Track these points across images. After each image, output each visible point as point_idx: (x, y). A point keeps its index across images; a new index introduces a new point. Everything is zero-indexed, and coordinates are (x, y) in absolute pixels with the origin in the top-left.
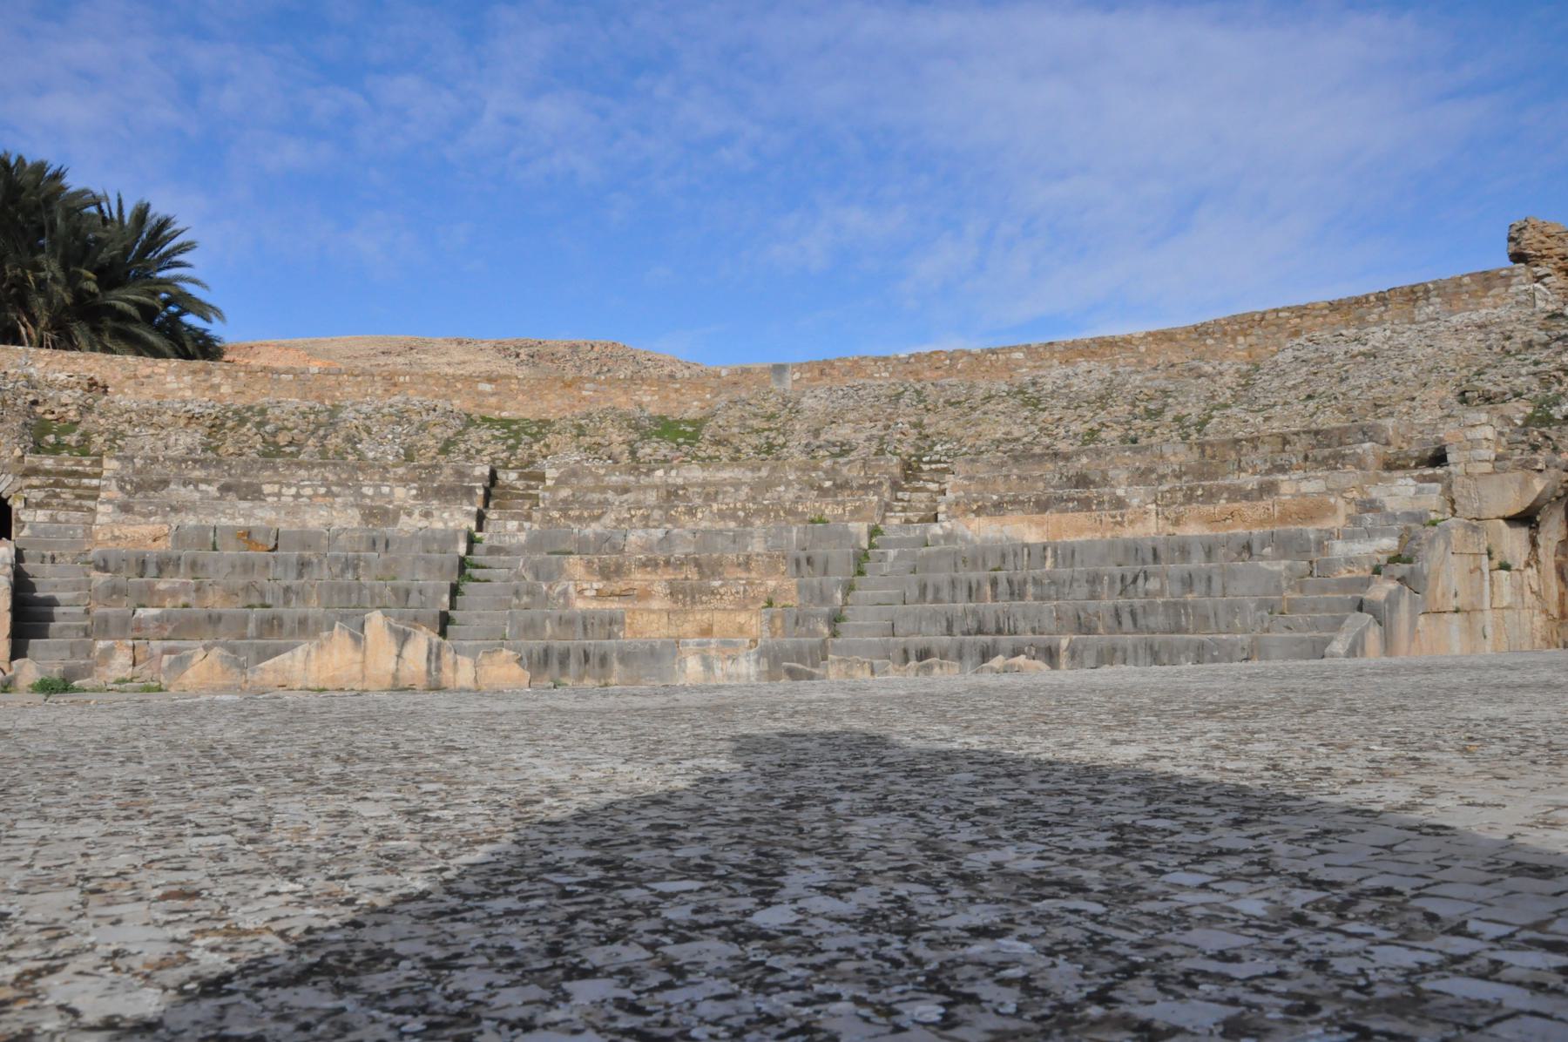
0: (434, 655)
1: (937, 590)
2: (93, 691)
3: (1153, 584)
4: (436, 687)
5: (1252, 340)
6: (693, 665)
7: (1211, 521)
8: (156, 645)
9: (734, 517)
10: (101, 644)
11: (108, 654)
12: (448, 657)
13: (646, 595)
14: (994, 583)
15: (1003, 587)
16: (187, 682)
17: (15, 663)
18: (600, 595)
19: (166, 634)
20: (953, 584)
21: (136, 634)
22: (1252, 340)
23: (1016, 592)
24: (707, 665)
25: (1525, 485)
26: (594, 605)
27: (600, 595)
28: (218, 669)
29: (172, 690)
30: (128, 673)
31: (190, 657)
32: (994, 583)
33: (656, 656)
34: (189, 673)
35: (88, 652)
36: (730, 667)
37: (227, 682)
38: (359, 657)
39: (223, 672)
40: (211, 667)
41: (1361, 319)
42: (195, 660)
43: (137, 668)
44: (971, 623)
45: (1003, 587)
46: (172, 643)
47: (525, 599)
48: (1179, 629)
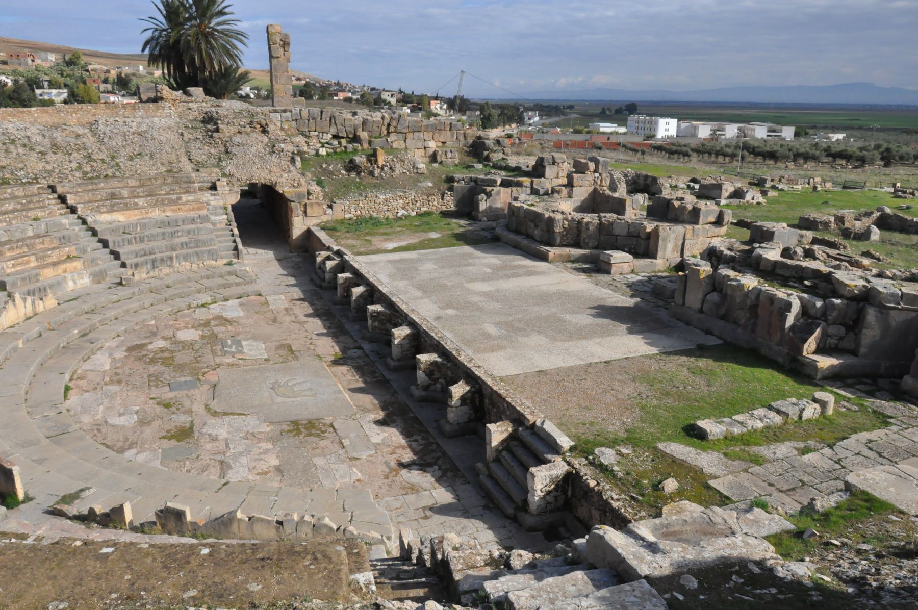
0: (33, 303)
3: (180, 234)
4: (36, 314)
5: (78, 116)
6: (71, 284)
7: (173, 211)
9: (5, 221)
12: (36, 303)
13: (28, 262)
14: (135, 238)
15: (138, 239)
18: (14, 266)
20: (123, 240)
22: (78, 116)
23: (142, 240)
24: (75, 283)
26: (13, 270)
27: (14, 266)
32: (135, 238)
33: (58, 284)
36: (82, 282)
41: (117, 113)
44: (142, 253)
45: (138, 239)
48: (198, 247)
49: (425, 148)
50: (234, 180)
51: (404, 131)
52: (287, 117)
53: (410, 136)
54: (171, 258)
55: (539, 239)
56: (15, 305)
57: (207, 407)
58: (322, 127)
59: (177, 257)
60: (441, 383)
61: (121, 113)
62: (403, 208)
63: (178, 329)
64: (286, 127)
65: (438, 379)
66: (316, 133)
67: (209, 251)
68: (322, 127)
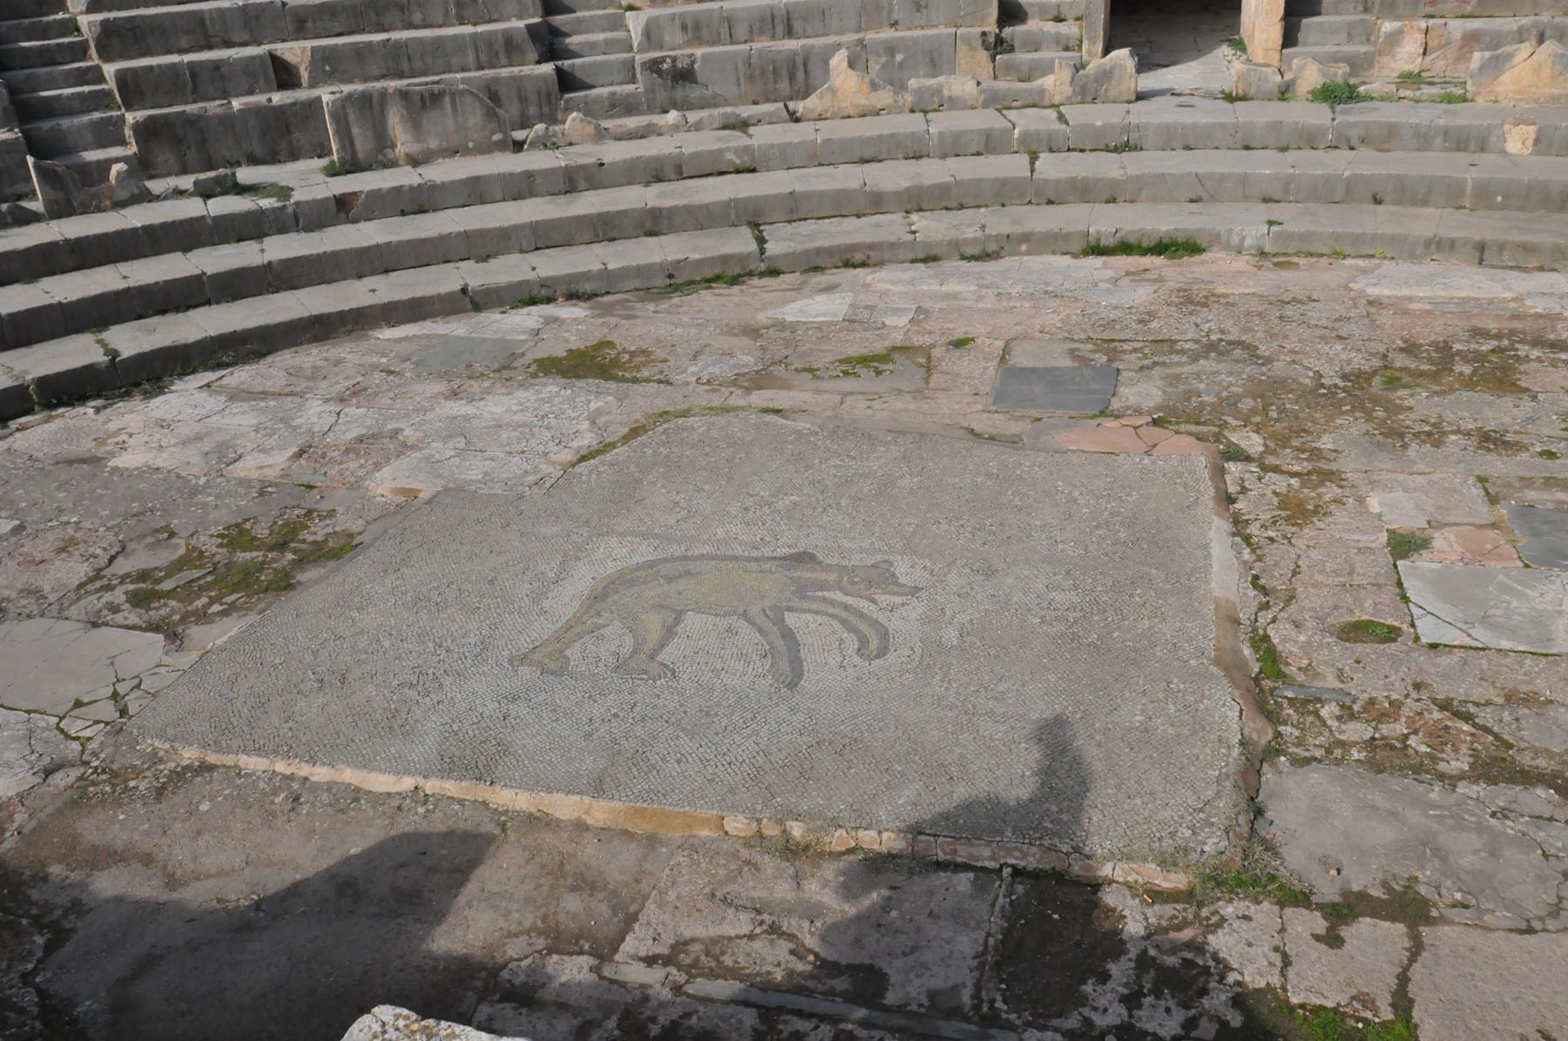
2: (1382, 99)
8: (1457, 27)
10: (1387, 26)
11: (1395, 39)
16: (1500, 89)
17: (1286, 51)
19: (1468, 9)
21: (1429, 10)
28: (1547, 72)
29: (1480, 100)
30: (1414, 66)
31: (1511, 55)
34: (1506, 77)
35: (1369, 33)
37: (1556, 92)
39: (1553, 77)
40: (1537, 71)
42: (1516, 59)
43: (1428, 58)
46: (1477, 24)
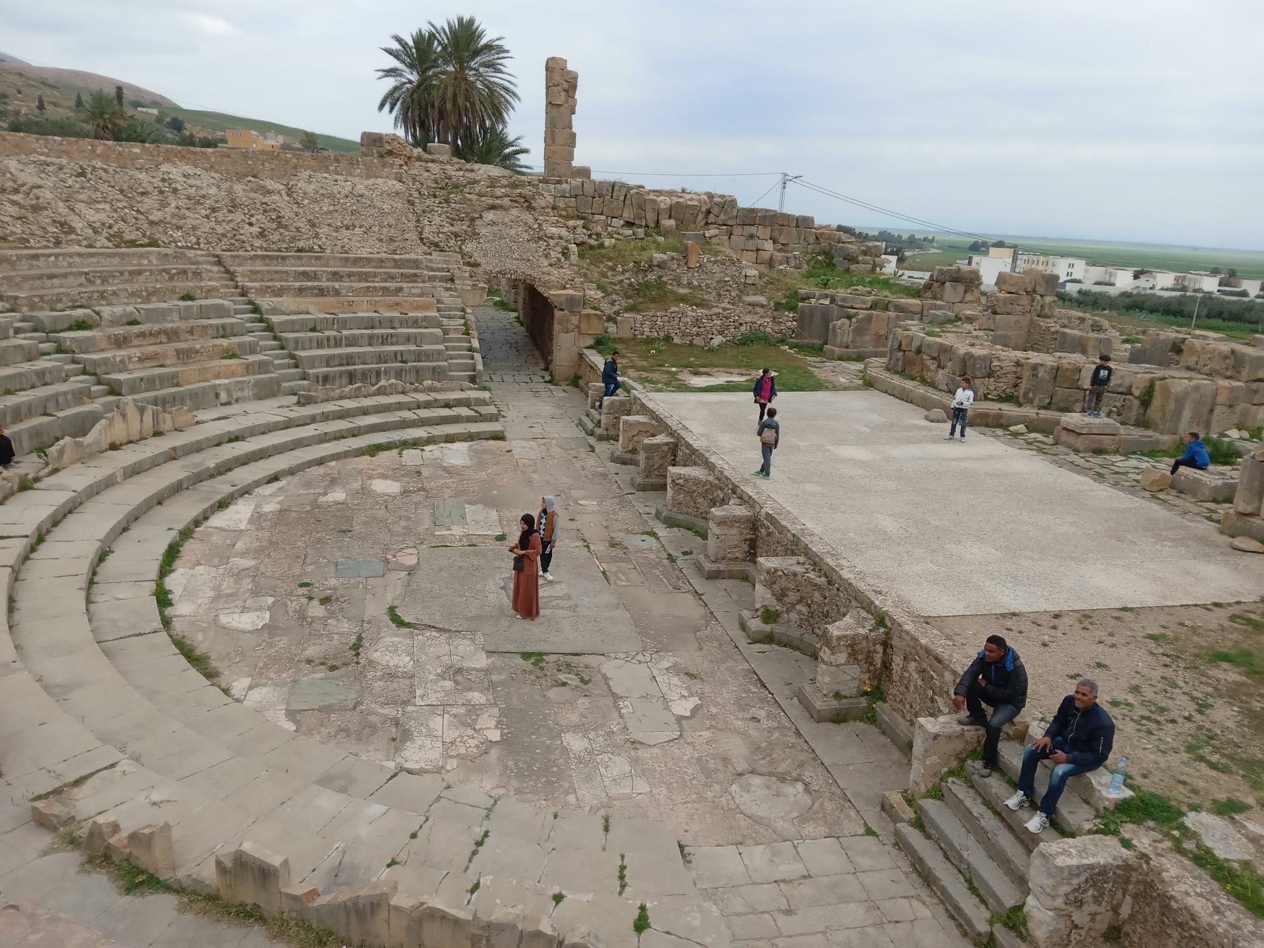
1: (303, 343)
25: (481, 296)
38: (125, 426)
41: (327, 167)
47: (103, 368)
49: (758, 250)
50: (480, 270)
51: (730, 223)
52: (564, 191)
53: (737, 230)
54: (378, 374)
55: (945, 388)
56: (124, 416)
57: (392, 610)
58: (612, 210)
59: (386, 372)
60: (800, 613)
61: (332, 168)
62: (721, 333)
63: (370, 478)
64: (561, 205)
65: (793, 605)
66: (603, 217)
67: (434, 368)
68: (612, 210)
